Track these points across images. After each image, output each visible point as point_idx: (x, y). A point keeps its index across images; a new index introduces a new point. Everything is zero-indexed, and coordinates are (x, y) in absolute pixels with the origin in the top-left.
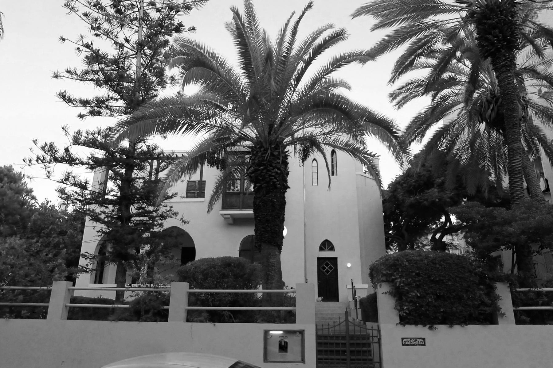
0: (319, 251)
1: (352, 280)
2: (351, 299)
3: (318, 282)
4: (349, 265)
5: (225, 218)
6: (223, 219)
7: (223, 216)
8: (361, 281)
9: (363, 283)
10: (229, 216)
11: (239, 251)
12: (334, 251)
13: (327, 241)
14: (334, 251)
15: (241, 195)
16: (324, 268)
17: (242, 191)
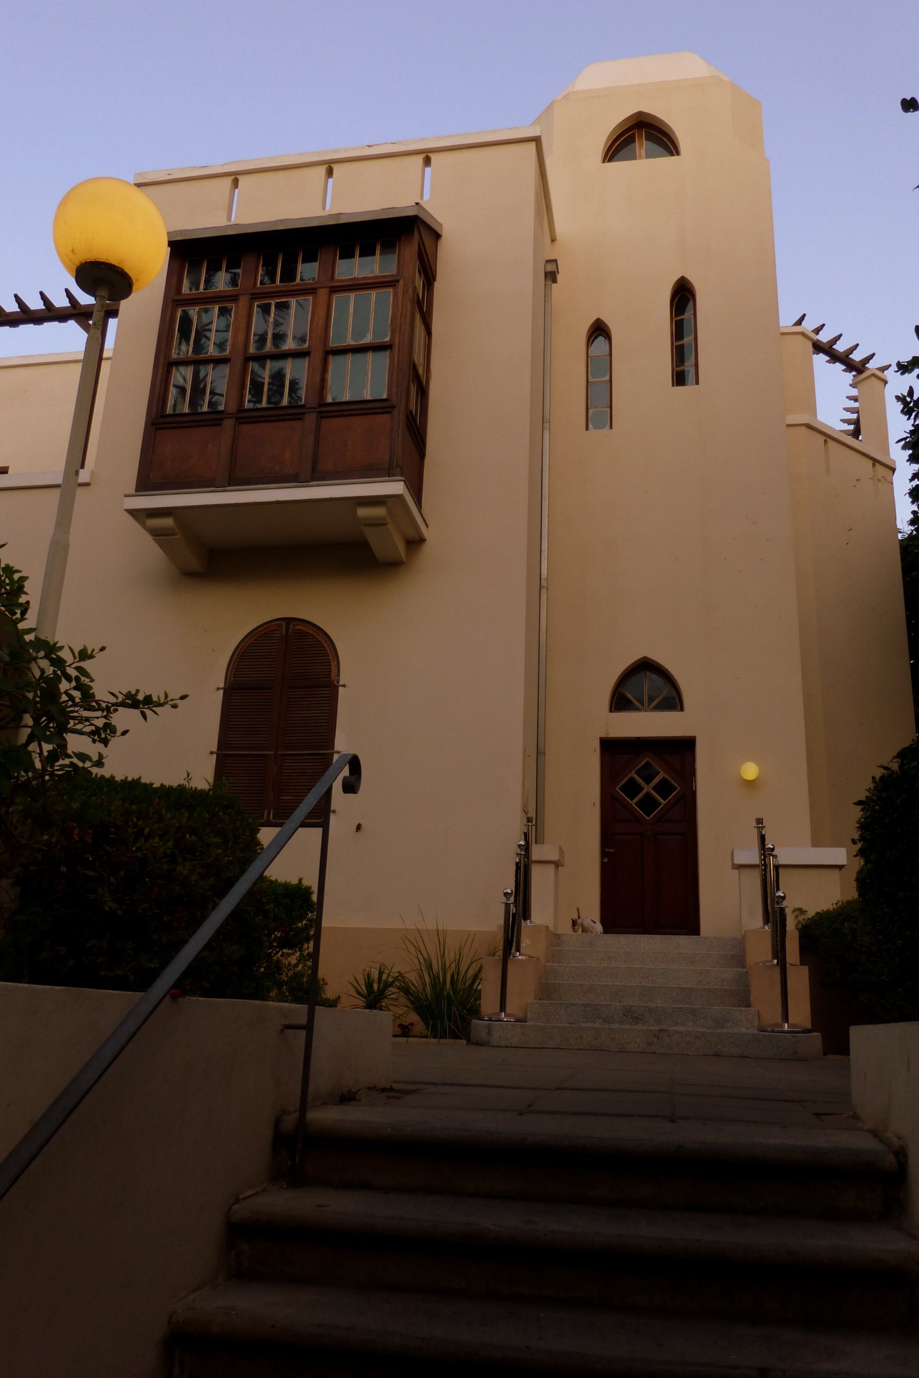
0: (611, 711)
1: (759, 821)
2: (754, 921)
3: (603, 854)
4: (750, 771)
5: (156, 533)
6: (149, 538)
7: (143, 525)
8: (805, 830)
9: (817, 842)
10: (168, 522)
11: (221, 692)
12: (682, 710)
13: (645, 666)
14: (682, 710)
15: (228, 424)
16: (632, 789)
17: (233, 408)
